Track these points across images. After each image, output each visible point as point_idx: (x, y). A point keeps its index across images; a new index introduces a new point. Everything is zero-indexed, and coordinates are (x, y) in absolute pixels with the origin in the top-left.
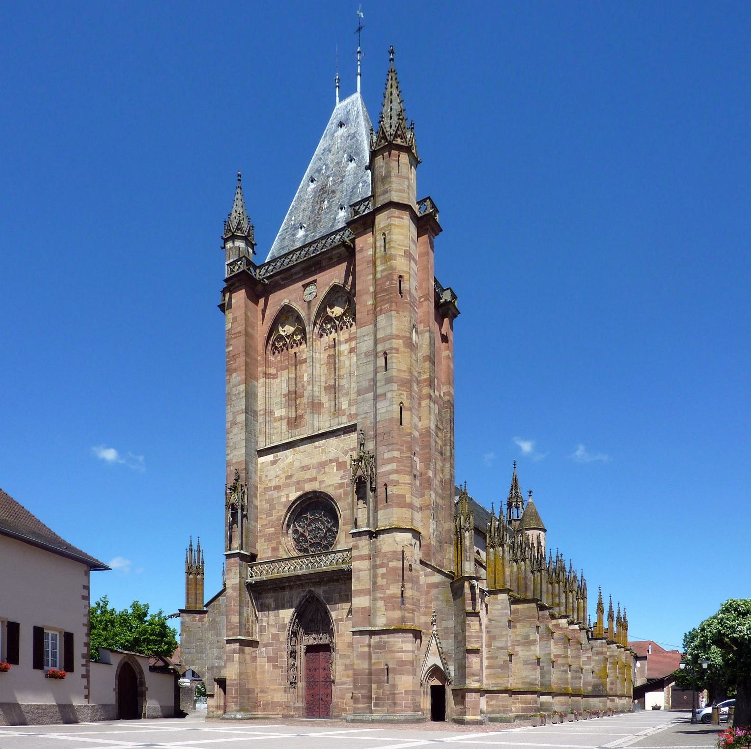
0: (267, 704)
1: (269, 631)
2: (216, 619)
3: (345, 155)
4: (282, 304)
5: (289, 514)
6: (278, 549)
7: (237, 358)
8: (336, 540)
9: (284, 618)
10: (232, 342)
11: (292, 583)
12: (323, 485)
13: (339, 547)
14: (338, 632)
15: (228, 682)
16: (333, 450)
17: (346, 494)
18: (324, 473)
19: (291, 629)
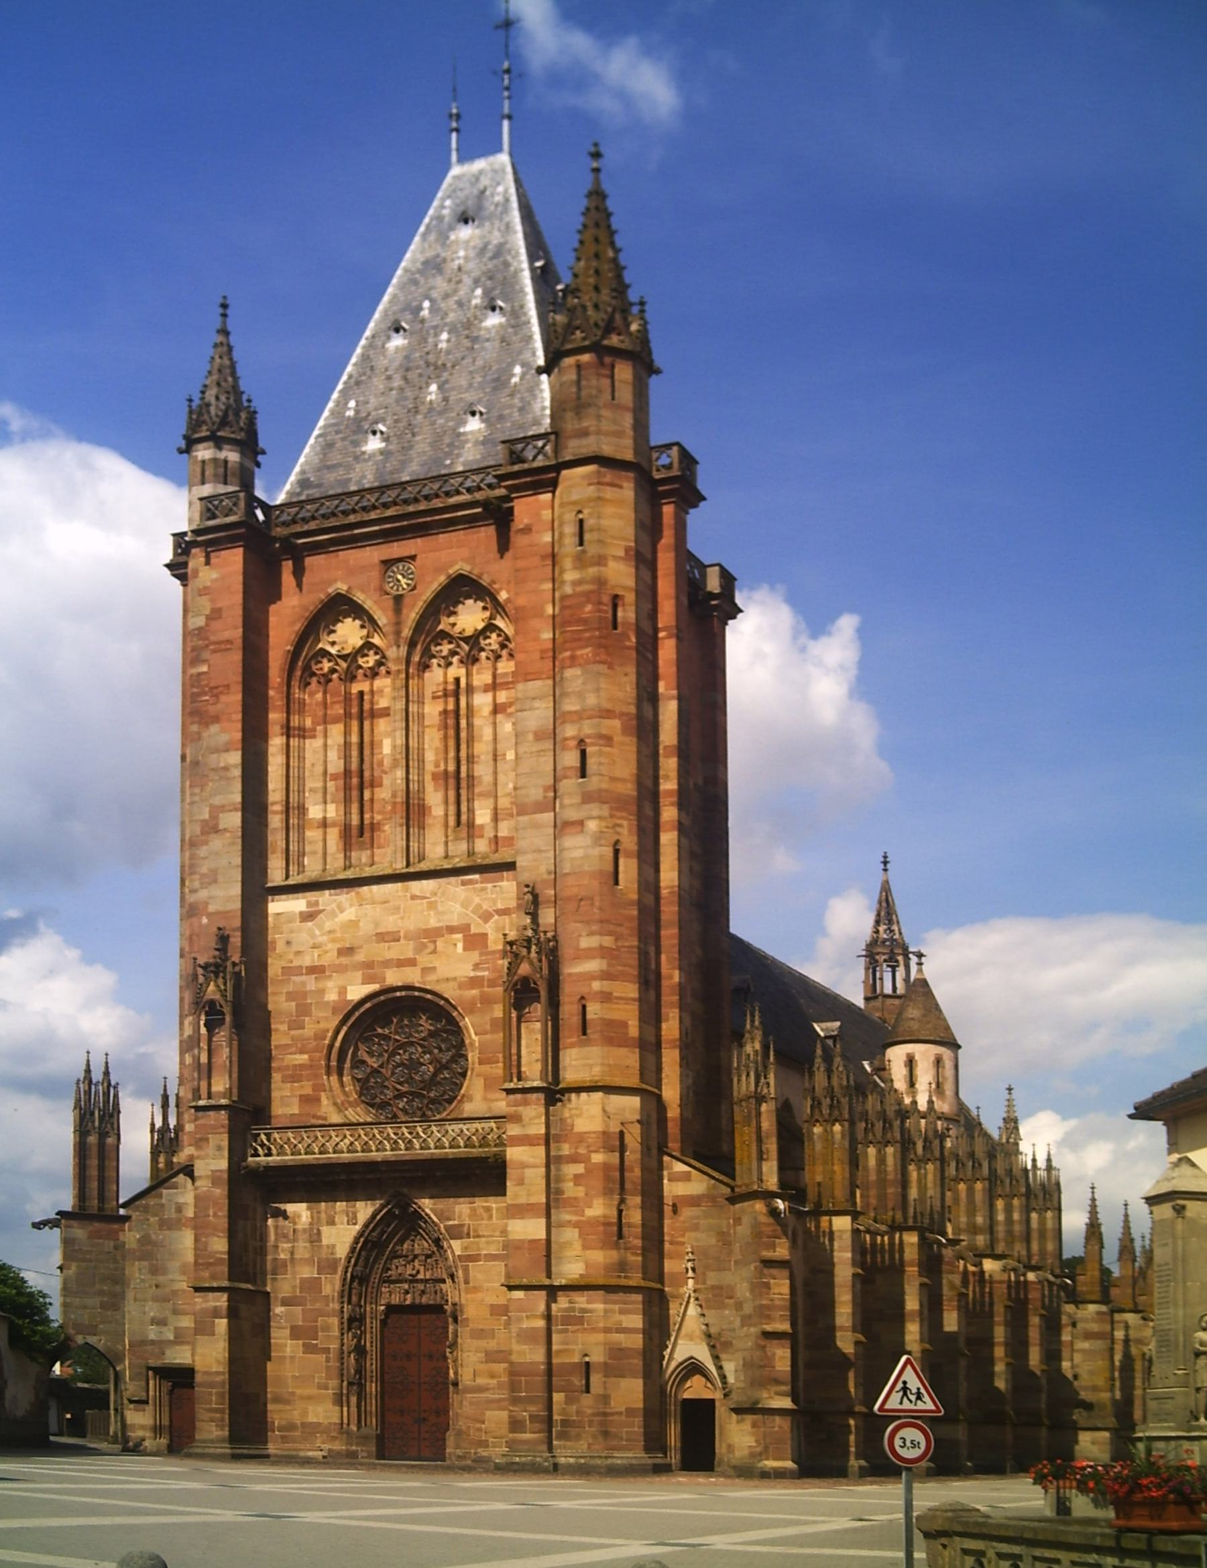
0: (291, 1427)
1: (294, 1273)
2: (153, 1237)
3: (479, 292)
4: (330, 590)
5: (345, 1029)
6: (318, 1100)
7: (221, 693)
8: (462, 1092)
9: (334, 1246)
10: (206, 655)
11: (356, 1177)
12: (432, 977)
13: (469, 1109)
15: (198, 1378)
16: (458, 908)
17: (487, 1001)
18: (434, 952)
19: (350, 1270)
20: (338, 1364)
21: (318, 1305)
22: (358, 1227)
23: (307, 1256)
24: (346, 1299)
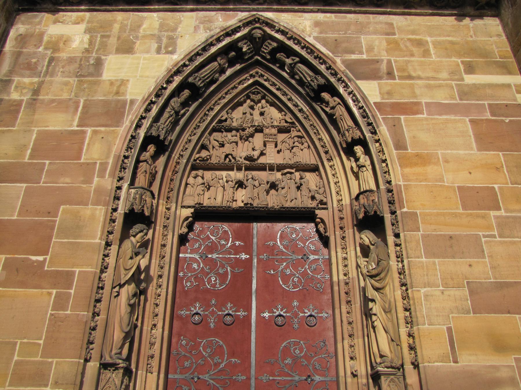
9: (123, 82)
14: (400, 145)
19: (146, 124)
20: (86, 314)
21: (65, 182)
22: (177, 57)
23: (65, 96)
24: (128, 174)
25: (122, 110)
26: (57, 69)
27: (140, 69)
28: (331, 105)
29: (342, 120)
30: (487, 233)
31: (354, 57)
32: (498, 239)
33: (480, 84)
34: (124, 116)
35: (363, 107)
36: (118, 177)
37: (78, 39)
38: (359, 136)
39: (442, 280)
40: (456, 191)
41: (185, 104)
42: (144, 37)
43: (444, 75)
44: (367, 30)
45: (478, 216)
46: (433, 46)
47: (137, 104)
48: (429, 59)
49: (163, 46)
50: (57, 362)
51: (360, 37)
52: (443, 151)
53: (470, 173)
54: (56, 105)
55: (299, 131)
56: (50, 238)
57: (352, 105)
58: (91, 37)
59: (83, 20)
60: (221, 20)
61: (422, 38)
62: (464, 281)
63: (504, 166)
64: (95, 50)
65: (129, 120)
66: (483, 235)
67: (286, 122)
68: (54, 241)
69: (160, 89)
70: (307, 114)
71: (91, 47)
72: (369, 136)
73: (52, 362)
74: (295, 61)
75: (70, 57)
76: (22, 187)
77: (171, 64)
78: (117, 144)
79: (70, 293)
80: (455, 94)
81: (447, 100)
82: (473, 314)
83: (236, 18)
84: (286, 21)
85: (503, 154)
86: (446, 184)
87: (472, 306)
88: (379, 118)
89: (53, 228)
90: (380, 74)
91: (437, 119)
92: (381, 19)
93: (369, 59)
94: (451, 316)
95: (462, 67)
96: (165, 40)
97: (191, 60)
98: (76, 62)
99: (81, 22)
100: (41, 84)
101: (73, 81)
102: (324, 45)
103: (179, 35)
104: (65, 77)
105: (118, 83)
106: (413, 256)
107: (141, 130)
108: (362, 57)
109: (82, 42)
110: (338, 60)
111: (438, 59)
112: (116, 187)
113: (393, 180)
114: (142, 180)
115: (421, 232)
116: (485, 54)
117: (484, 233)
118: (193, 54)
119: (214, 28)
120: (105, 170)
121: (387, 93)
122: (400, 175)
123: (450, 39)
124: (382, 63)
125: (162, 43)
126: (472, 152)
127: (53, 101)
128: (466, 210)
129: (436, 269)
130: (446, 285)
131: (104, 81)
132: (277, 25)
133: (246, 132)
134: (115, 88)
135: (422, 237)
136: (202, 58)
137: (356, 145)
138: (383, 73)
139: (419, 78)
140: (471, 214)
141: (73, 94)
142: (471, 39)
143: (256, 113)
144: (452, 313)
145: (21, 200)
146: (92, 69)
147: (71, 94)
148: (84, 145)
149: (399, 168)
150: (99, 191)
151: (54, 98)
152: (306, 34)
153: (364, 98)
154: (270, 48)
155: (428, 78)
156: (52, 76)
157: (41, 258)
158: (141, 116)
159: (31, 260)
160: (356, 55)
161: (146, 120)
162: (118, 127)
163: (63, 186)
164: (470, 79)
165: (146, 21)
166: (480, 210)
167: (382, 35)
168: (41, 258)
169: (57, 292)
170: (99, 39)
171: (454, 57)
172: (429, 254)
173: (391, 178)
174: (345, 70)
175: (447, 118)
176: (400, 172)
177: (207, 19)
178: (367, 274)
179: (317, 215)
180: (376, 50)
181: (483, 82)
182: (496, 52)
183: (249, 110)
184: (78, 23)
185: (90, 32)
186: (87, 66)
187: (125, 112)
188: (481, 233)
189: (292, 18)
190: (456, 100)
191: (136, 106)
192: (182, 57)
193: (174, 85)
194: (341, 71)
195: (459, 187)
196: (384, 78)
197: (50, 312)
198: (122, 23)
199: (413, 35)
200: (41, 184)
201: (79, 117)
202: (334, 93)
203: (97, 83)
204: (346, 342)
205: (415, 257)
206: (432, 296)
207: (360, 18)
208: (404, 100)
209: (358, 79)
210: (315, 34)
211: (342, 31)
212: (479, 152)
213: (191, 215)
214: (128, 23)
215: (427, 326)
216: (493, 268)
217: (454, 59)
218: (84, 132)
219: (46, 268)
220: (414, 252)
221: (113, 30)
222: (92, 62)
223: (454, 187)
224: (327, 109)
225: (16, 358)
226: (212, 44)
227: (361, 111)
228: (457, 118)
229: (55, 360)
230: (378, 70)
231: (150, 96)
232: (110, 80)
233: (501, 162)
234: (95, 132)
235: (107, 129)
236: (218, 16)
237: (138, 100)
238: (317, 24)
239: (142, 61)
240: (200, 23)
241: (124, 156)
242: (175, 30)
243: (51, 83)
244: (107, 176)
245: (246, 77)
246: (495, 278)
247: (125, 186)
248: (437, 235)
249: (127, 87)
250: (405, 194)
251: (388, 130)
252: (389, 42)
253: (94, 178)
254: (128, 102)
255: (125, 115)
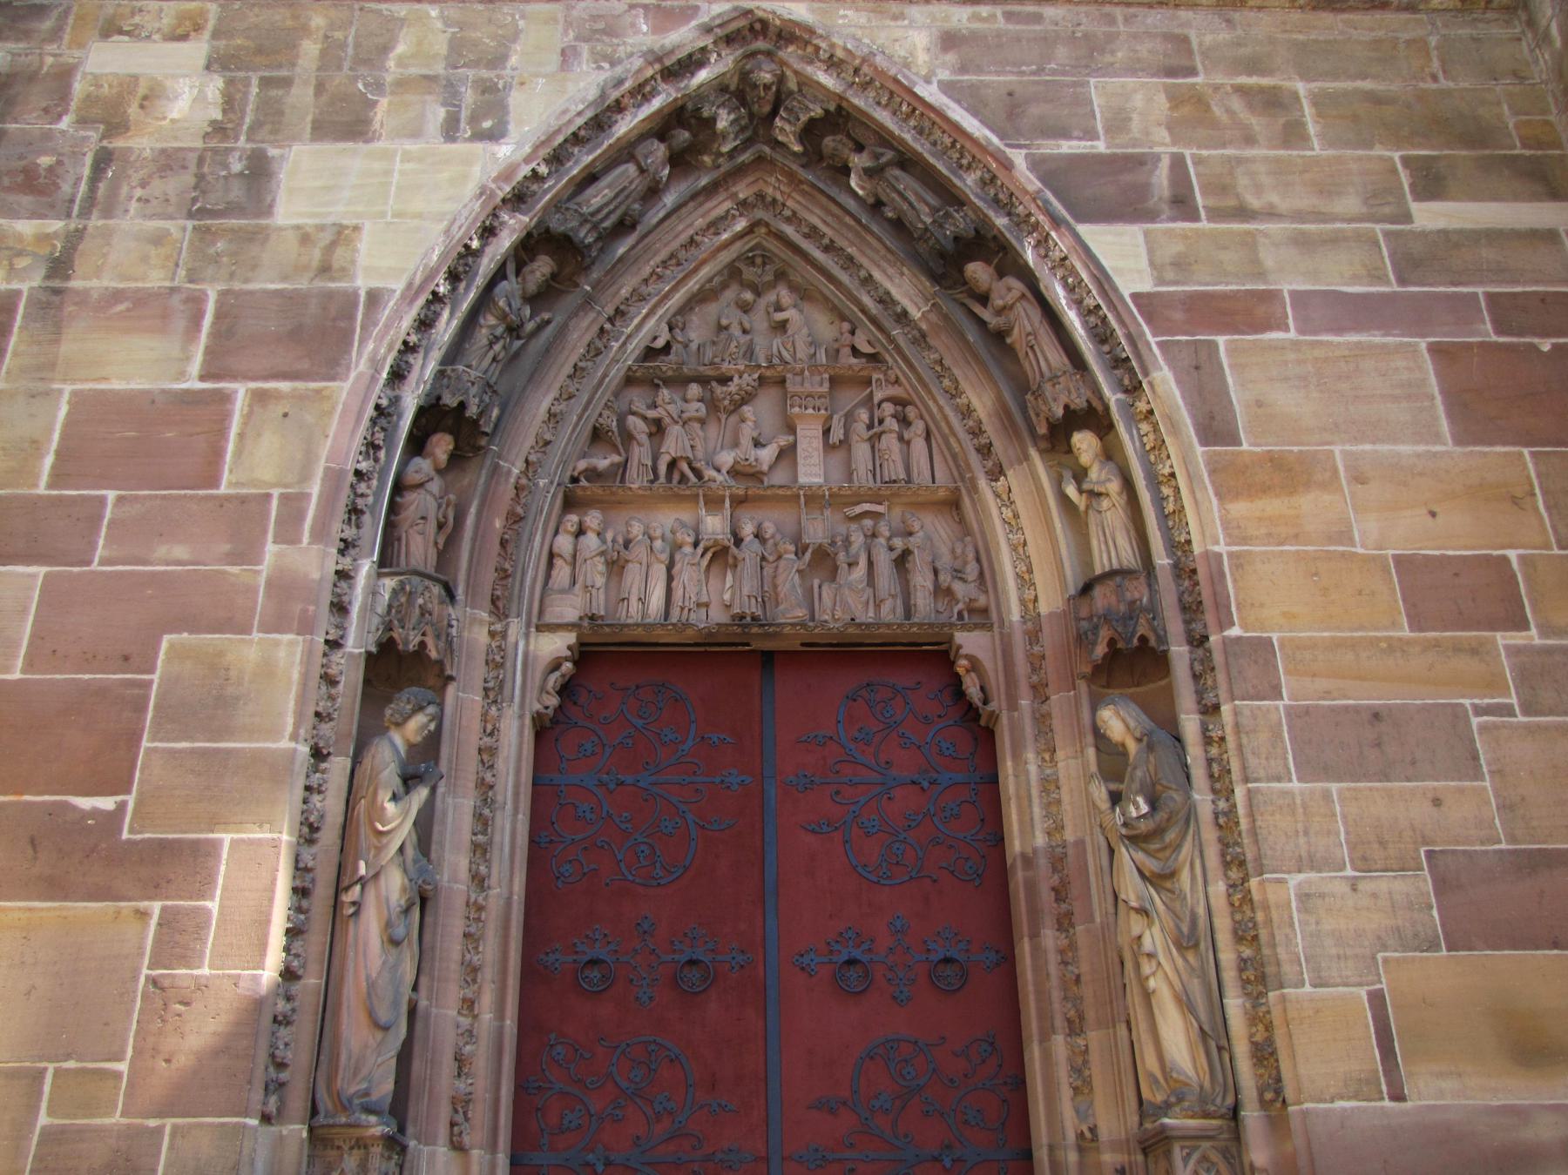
9: (342, 235)
23: (156, 279)
24: (373, 531)
25: (342, 324)
26: (125, 190)
27: (393, 189)
28: (999, 303)
29: (1032, 347)
30: (1487, 701)
31: (1067, 147)
32: (1521, 719)
33: (1461, 232)
34: (351, 344)
35: (1098, 307)
36: (341, 540)
37: (187, 89)
38: (1088, 401)
39: (1352, 847)
40: (1390, 573)
41: (540, 298)
42: (402, 84)
43: (1350, 203)
44: (1108, 58)
45: (1457, 648)
46: (1313, 110)
47: (391, 304)
48: (1302, 153)
49: (464, 115)
50: (175, 1128)
51: (1086, 84)
52: (1348, 447)
53: (1433, 514)
54: (128, 310)
55: (897, 381)
56: (134, 738)
57: (1063, 302)
58: (230, 82)
59: (198, 28)
60: (645, 28)
61: (1281, 83)
62: (1417, 850)
63: (1537, 491)
64: (245, 127)
65: (365, 357)
66: (1475, 706)
67: (855, 352)
68: (148, 749)
69: (461, 256)
70: (920, 330)
71: (232, 116)
72: (1117, 400)
73: (159, 1131)
74: (883, 160)
75: (163, 151)
76: (34, 576)
77: (494, 174)
78: (331, 434)
79: (208, 912)
80: (1383, 262)
81: (1361, 285)
82: (1449, 950)
83: (694, 23)
84: (853, 29)
85: (1532, 453)
86: (1360, 550)
87: (1443, 925)
88: (1148, 344)
89: (141, 707)
90: (1151, 203)
91: (1329, 343)
92: (1149, 21)
93: (1115, 155)
94: (1380, 956)
95: (1405, 178)
96: (469, 97)
97: (557, 159)
98: (184, 167)
99: (192, 34)
100: (74, 239)
101: (180, 229)
102: (974, 112)
103: (512, 77)
104: (152, 217)
105: (326, 238)
106: (1262, 773)
107: (406, 388)
108: (1092, 147)
109: (200, 99)
110: (1018, 158)
111: (1331, 152)
112: (337, 572)
113: (1195, 538)
114: (419, 548)
115: (1287, 702)
116: (1476, 135)
117: (1476, 701)
118: (560, 139)
119: (623, 55)
120: (300, 516)
121: (1172, 264)
122: (1218, 522)
123: (1367, 85)
124: (1157, 167)
125: (459, 106)
126: (1438, 448)
127: (117, 296)
128: (1421, 630)
129: (1334, 815)
130: (1364, 864)
131: (281, 229)
132: (823, 45)
133: (732, 387)
134: (317, 255)
135: (1288, 715)
136: (588, 153)
137: (1080, 428)
138: (1160, 199)
139: (1271, 214)
140: (1437, 644)
141: (182, 273)
142: (1434, 86)
143: (758, 321)
144: (1385, 948)
145: (31, 618)
146: (237, 192)
147: (174, 274)
148: (227, 440)
149: (1215, 501)
150: (283, 587)
151: (121, 286)
152: (916, 74)
153: (1102, 279)
154: (804, 118)
155: (1299, 216)
156: (108, 213)
157: (107, 803)
158: (405, 343)
159: (74, 808)
160: (1074, 143)
161: (421, 355)
162: (333, 379)
163: (166, 572)
164: (1430, 216)
165: (405, 30)
166: (1463, 629)
167: (1153, 76)
168: (107, 803)
169: (164, 909)
170: (254, 90)
171: (1381, 143)
172: (1312, 768)
173: (1188, 533)
174: (1040, 191)
175: (1360, 343)
176: (1217, 515)
177: (601, 25)
178: (1124, 831)
179: (960, 647)
180: (1136, 125)
181: (1469, 226)
182: (1511, 125)
183: (733, 318)
184: (184, 38)
185: (225, 68)
186: (222, 181)
187: (353, 331)
188: (1467, 702)
189: (869, 20)
190: (1388, 283)
191: (387, 312)
192: (527, 149)
193: (505, 241)
194: (1026, 192)
195: (1398, 560)
196: (1164, 217)
197: (145, 971)
198: (326, 37)
199: (1250, 75)
200: (95, 566)
201: (207, 348)
202: (1007, 262)
203: (257, 236)
204: (1059, 1042)
205: (1270, 779)
206: (1322, 896)
207: (1084, 20)
208: (1227, 284)
209: (1083, 218)
210: (944, 75)
211: (1028, 65)
212: (1459, 449)
213: (569, 653)
214: (346, 38)
215: (1308, 988)
216: (1505, 807)
217: (1379, 151)
218: (225, 398)
219: (125, 835)
220: (1263, 761)
221: (300, 62)
222: (237, 167)
223: (1385, 557)
224: (986, 315)
225: (43, 1119)
226: (618, 107)
227: (1092, 320)
228: (1390, 339)
229: (169, 1122)
230: (1143, 190)
231: (430, 276)
232: (298, 227)
233: (1528, 477)
234: (260, 398)
235: (300, 385)
236: (636, 16)
237: (395, 291)
238: (949, 40)
239: (398, 166)
240: (577, 38)
241: (358, 473)
242: (498, 61)
243: (107, 235)
244: (306, 538)
245: (728, 211)
246: (1512, 839)
247: (366, 567)
248: (1332, 709)
249: (355, 250)
250: (1235, 581)
251: (1179, 382)
252: (1176, 99)
253: (263, 544)
254: (362, 299)
255: (353, 340)
